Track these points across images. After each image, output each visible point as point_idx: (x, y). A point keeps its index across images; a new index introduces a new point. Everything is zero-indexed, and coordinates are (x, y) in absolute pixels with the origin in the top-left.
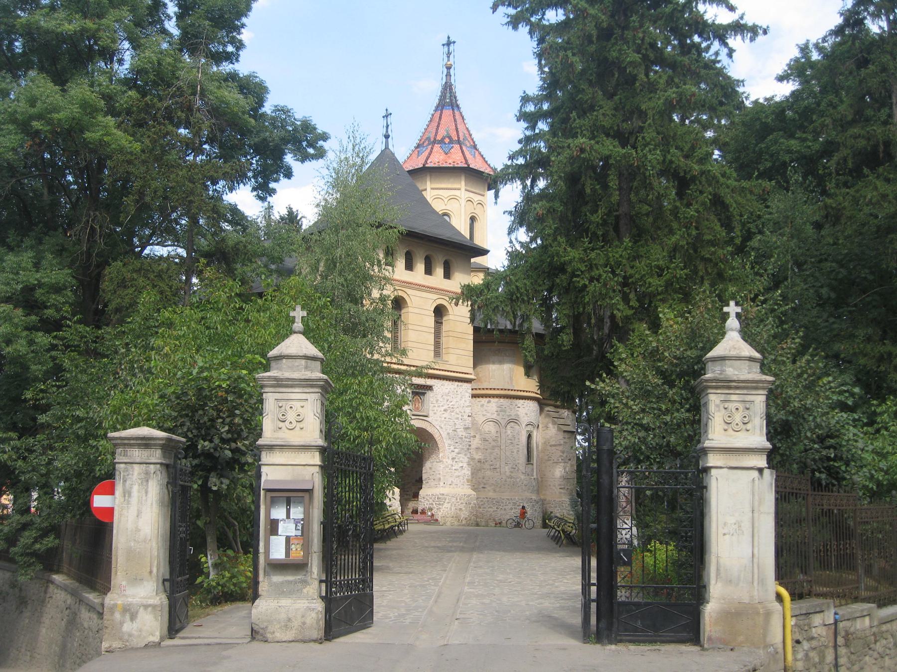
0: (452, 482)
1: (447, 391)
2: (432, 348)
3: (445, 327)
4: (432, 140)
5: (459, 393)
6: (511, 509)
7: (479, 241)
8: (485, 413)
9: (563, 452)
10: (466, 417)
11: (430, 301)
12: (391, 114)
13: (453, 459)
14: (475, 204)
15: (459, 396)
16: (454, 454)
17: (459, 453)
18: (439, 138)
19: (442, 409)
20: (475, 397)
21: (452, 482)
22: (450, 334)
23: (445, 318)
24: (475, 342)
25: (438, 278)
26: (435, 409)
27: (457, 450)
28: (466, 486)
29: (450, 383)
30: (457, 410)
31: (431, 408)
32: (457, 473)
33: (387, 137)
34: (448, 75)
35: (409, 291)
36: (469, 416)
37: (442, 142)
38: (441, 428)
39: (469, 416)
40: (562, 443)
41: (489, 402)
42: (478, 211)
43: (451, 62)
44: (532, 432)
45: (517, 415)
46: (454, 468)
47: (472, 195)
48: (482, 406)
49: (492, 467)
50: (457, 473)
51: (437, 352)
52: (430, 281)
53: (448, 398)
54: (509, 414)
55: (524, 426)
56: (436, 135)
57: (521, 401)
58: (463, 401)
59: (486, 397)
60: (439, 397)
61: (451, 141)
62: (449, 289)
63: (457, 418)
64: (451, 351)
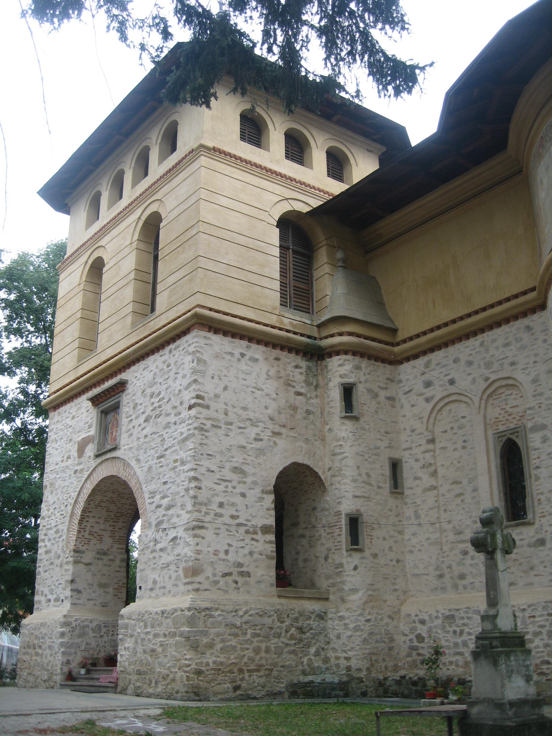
0: (155, 582)
17: (168, 508)
19: (143, 417)
21: (155, 582)
28: (182, 588)
31: (124, 428)
38: (138, 460)
46: (159, 546)
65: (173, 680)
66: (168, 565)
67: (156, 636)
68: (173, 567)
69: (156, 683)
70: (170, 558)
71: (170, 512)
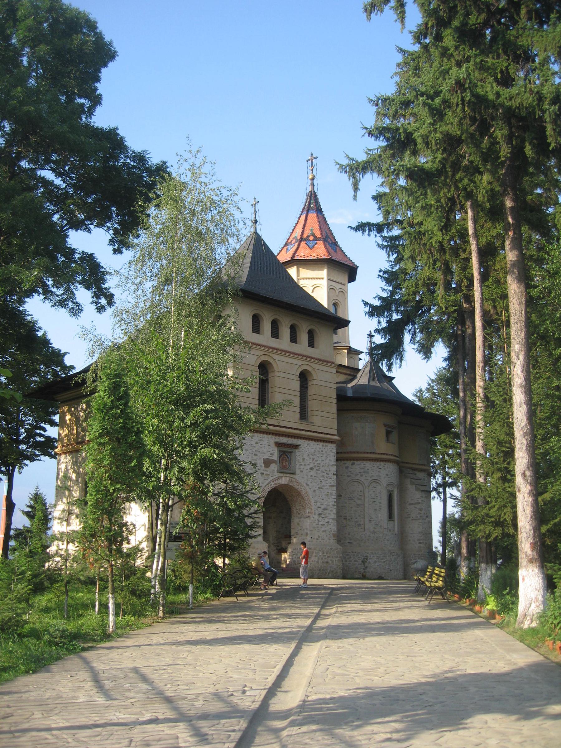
0: (319, 537)
1: (313, 451)
2: (298, 410)
3: (312, 391)
4: (299, 238)
5: (324, 453)
6: (375, 562)
7: (340, 314)
8: (349, 474)
9: (421, 510)
10: (331, 475)
11: (297, 366)
12: (258, 202)
13: (320, 514)
14: (337, 292)
15: (325, 456)
16: (320, 511)
17: (325, 509)
18: (305, 236)
19: (309, 467)
20: (341, 460)
21: (319, 537)
22: (315, 397)
23: (310, 383)
24: (338, 410)
25: (302, 346)
26: (302, 467)
27: (323, 507)
29: (316, 443)
30: (323, 469)
31: (297, 466)
32: (323, 528)
33: (256, 222)
34: (313, 185)
35: (276, 357)
36: (334, 474)
37: (307, 239)
38: (308, 485)
39: (334, 474)
40: (420, 501)
41: (353, 464)
42: (340, 299)
43: (315, 173)
44: (393, 491)
45: (379, 476)
46: (320, 523)
47: (333, 284)
48: (347, 467)
49: (357, 524)
50: (323, 528)
51: (304, 414)
52: (294, 348)
53: (314, 457)
54: (371, 475)
55: (385, 485)
56: (302, 233)
57: (382, 464)
58: (327, 461)
59: (350, 460)
60: (305, 456)
61: (316, 239)
62: (313, 356)
63: (323, 476)
64: (316, 413)
65: (337, 572)
66: (325, 531)
67: (328, 557)
68: (328, 533)
69: (329, 573)
70: (326, 529)
71: (325, 511)
